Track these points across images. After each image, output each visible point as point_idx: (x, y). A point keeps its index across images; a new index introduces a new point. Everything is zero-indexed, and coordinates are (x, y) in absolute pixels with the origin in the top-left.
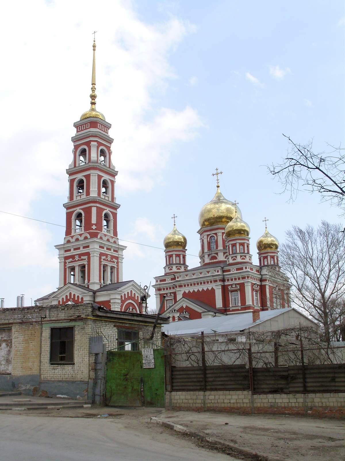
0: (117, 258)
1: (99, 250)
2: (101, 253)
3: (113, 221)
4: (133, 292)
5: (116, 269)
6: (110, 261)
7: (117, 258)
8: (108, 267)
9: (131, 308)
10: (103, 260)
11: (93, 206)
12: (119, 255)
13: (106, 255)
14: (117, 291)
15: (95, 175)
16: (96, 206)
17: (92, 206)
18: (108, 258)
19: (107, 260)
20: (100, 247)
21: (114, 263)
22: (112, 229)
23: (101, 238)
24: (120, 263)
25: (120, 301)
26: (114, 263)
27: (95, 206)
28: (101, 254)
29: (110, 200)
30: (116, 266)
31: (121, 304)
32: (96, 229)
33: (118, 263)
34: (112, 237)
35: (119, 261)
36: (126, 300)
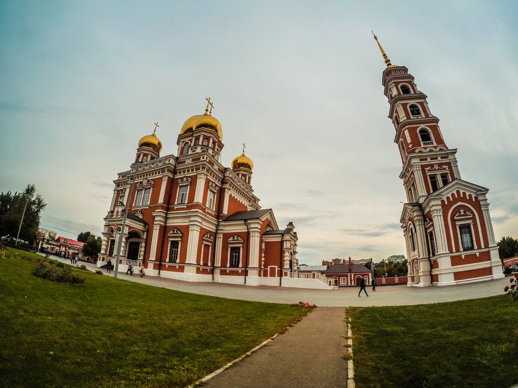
0: (449, 164)
1: (420, 163)
2: (422, 166)
3: (432, 133)
4: (461, 192)
5: (449, 175)
6: (439, 169)
7: (449, 164)
8: (438, 176)
9: (462, 211)
10: (428, 171)
11: (405, 130)
12: (450, 160)
13: (432, 166)
14: (433, 196)
15: (399, 106)
16: (407, 128)
17: (404, 130)
18: (435, 167)
19: (435, 170)
20: (421, 160)
21: (446, 169)
22: (434, 139)
23: (420, 152)
24: (453, 168)
25: (440, 207)
26: (446, 169)
27: (406, 129)
28: (423, 167)
29: (424, 116)
30: (448, 172)
31: (443, 210)
32: (412, 147)
33: (450, 168)
34: (436, 147)
35: (452, 165)
36: (451, 204)
